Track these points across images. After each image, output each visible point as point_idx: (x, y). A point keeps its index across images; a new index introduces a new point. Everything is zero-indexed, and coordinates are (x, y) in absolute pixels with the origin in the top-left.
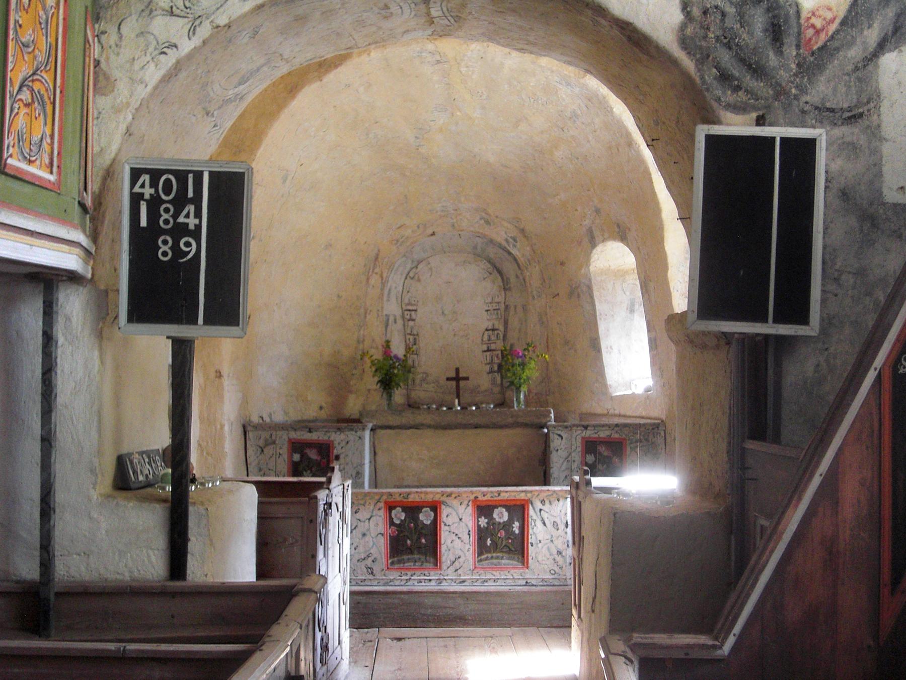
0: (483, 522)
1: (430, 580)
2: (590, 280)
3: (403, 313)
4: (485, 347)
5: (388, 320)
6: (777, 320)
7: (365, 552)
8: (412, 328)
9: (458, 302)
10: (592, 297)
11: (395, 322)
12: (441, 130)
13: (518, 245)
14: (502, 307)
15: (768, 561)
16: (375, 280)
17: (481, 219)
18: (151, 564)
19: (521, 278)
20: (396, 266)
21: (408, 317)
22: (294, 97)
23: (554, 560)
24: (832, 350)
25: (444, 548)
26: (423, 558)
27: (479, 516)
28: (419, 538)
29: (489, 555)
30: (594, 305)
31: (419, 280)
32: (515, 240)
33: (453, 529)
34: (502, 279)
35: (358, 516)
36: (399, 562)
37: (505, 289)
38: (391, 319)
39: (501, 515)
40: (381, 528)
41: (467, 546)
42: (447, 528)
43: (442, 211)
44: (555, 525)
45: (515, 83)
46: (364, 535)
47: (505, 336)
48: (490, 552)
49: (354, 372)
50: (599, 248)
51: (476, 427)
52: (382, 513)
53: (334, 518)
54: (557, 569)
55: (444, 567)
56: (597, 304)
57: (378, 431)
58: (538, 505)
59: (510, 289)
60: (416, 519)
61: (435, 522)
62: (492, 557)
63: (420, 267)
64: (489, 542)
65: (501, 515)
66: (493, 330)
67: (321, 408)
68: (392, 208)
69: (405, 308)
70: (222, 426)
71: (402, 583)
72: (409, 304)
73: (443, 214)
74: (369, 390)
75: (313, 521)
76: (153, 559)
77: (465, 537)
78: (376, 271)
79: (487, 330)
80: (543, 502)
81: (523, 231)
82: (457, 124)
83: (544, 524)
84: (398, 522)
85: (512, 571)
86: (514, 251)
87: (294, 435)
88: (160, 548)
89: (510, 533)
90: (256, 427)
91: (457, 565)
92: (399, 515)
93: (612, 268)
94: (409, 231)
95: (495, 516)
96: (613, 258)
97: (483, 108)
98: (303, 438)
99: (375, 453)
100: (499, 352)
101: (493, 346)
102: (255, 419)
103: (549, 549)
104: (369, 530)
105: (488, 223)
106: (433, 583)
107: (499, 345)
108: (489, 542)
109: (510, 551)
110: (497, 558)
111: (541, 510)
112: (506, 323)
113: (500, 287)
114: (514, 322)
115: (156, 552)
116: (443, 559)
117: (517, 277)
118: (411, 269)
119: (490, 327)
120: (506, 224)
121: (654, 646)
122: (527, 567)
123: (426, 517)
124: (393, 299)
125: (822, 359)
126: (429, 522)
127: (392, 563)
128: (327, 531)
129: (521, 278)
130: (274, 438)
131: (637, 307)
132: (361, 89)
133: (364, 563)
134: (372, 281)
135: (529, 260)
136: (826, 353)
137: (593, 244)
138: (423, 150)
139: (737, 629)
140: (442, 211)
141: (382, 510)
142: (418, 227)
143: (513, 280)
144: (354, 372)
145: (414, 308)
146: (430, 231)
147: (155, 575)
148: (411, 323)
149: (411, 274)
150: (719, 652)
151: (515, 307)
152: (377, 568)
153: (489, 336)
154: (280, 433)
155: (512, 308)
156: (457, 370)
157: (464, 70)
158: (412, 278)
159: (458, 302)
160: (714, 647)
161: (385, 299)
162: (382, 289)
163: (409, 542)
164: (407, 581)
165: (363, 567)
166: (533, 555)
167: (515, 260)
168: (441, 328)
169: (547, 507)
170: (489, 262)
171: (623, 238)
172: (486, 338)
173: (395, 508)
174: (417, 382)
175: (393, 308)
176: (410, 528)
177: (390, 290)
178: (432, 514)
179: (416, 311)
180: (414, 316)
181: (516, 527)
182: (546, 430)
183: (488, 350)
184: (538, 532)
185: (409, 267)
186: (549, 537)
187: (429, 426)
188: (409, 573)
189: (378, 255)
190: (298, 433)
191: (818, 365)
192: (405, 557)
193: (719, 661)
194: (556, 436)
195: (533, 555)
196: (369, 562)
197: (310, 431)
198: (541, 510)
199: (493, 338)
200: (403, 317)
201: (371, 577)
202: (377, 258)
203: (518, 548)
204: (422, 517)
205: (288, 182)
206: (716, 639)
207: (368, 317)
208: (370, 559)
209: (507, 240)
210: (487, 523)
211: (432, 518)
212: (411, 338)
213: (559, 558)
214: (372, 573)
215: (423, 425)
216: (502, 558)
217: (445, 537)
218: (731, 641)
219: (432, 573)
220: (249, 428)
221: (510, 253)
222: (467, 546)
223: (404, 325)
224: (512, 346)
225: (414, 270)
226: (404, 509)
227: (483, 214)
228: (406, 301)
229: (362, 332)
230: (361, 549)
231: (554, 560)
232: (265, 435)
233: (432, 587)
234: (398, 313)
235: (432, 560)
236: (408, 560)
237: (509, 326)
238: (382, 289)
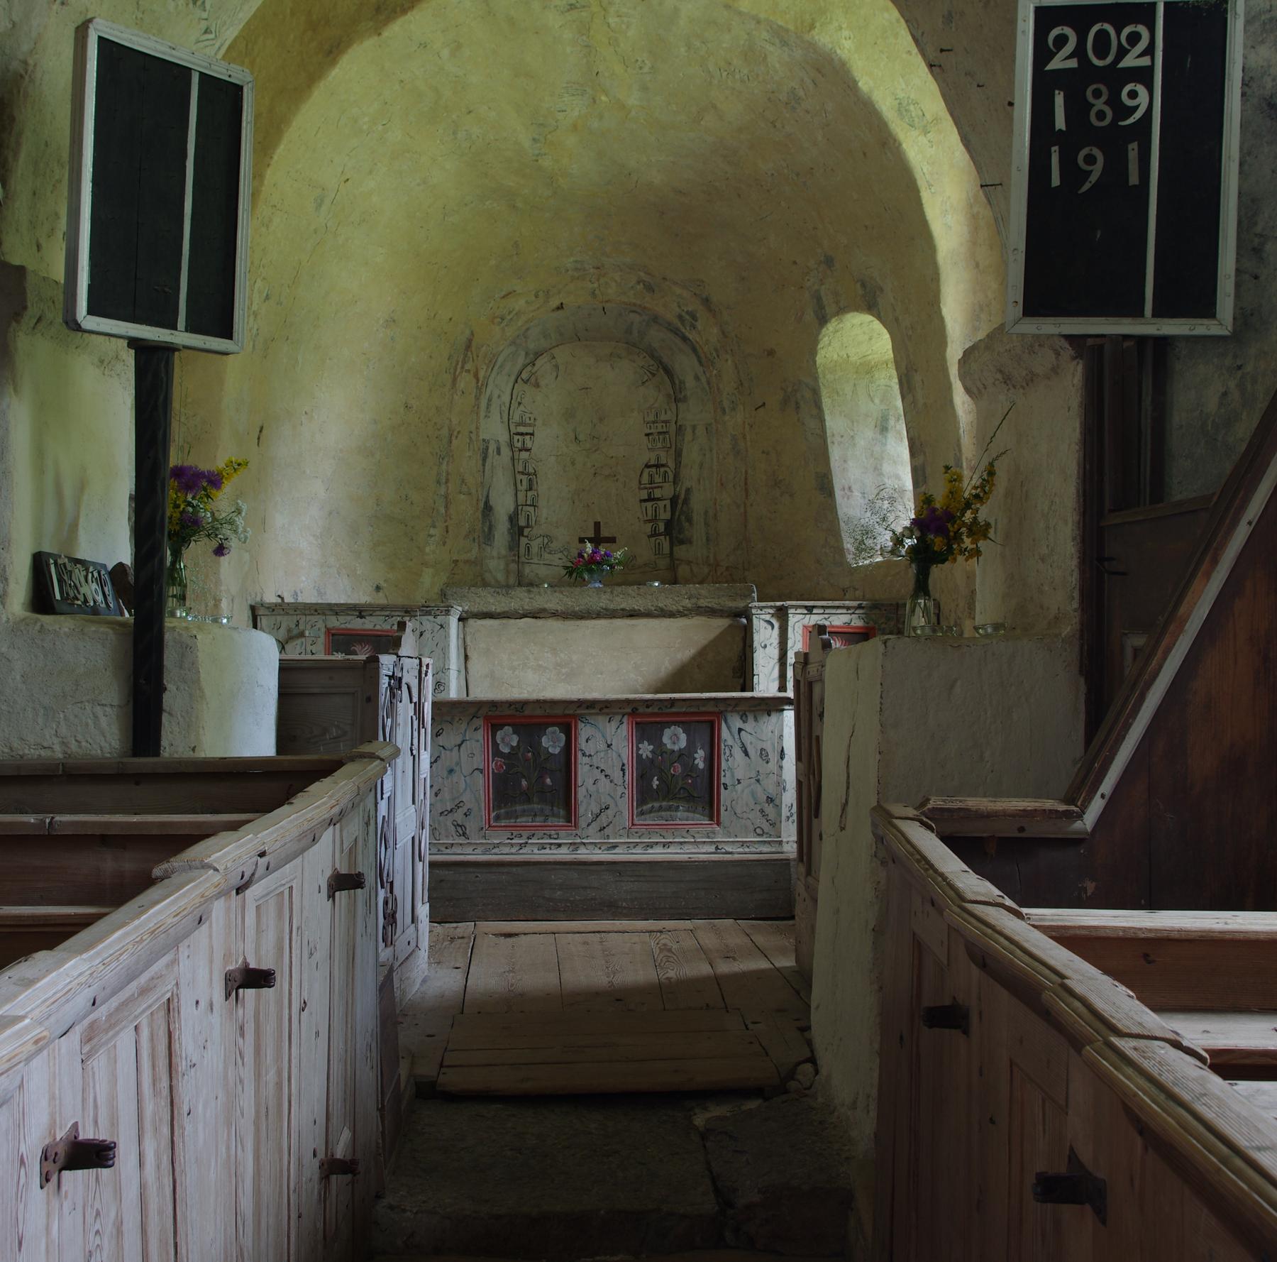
0: (646, 749)
1: (559, 845)
2: (816, 379)
3: (511, 439)
4: (644, 495)
5: (487, 448)
6: (1156, 314)
7: (453, 799)
8: (526, 462)
9: (601, 420)
10: (818, 405)
11: (499, 453)
12: (575, 127)
13: (699, 325)
14: (673, 428)
15: (1160, 667)
16: (465, 381)
17: (638, 283)
18: (99, 733)
19: (703, 380)
20: (501, 359)
21: (520, 445)
22: (333, 63)
23: (762, 811)
24: (1249, 368)
25: (581, 793)
26: (547, 808)
27: (640, 741)
28: (541, 777)
29: (656, 805)
30: (822, 421)
31: (537, 385)
32: (694, 318)
33: (595, 761)
34: (673, 383)
35: (441, 740)
36: (508, 816)
37: (676, 400)
38: (492, 447)
39: (675, 739)
40: (479, 761)
41: (620, 790)
42: (586, 760)
43: (576, 269)
44: (763, 753)
45: (698, 44)
46: (451, 771)
47: (676, 476)
48: (656, 800)
49: (432, 531)
50: (831, 326)
51: (633, 614)
52: (480, 735)
53: (405, 710)
54: (766, 826)
55: (583, 823)
56: (827, 417)
57: (471, 622)
58: (736, 722)
59: (685, 400)
60: (535, 747)
61: (568, 749)
62: (660, 809)
63: (539, 363)
64: (655, 783)
65: (675, 739)
66: (657, 466)
67: (378, 588)
68: (493, 262)
69: (513, 430)
70: (217, 602)
71: (513, 850)
72: (518, 425)
73: (576, 274)
74: (456, 562)
75: (372, 699)
76: (103, 721)
77: (617, 775)
78: (467, 367)
79: (647, 466)
80: (744, 718)
81: (706, 301)
82: (601, 117)
83: (746, 753)
84: (506, 750)
85: (693, 830)
86: (691, 335)
87: (335, 622)
88: (116, 702)
89: (690, 769)
90: (272, 609)
91: (603, 819)
92: (509, 739)
93: (853, 359)
94: (522, 302)
95: (666, 740)
96: (859, 342)
97: (644, 88)
98: (349, 626)
99: (466, 657)
100: (668, 503)
101: (657, 493)
102: (271, 598)
103: (753, 794)
104: (458, 764)
105: (650, 288)
106: (564, 850)
107: (667, 491)
108: (655, 783)
109: (690, 798)
110: (669, 809)
111: (740, 730)
112: (678, 454)
113: (669, 396)
114: (692, 453)
115: (108, 709)
116: (581, 810)
117: (697, 378)
118: (526, 366)
119: (652, 462)
120: (678, 291)
121: (967, 814)
122: (718, 824)
123: (552, 742)
124: (495, 410)
125: (1232, 384)
126: (557, 751)
127: (498, 818)
128: (395, 725)
129: (703, 380)
130: (301, 627)
131: (892, 422)
132: (445, 53)
133: (450, 817)
134: (461, 385)
135: (716, 350)
136: (1240, 373)
137: (823, 320)
138: (546, 163)
139: (1107, 786)
140: (576, 269)
141: (481, 732)
142: (536, 296)
143: (690, 383)
144: (432, 531)
145: (529, 430)
146: (556, 303)
147: (107, 749)
148: (524, 455)
149: (524, 376)
150: (1078, 825)
151: (694, 428)
152: (471, 826)
153: (651, 476)
154: (314, 618)
155: (689, 430)
156: (597, 525)
157: (612, 20)
158: (526, 382)
159: (601, 420)
160: (1067, 814)
161: (482, 414)
162: (477, 398)
163: (524, 783)
164: (521, 846)
165: (449, 824)
166: (728, 803)
167: (694, 350)
168: (573, 463)
169: (749, 726)
170: (652, 357)
171: (870, 306)
172: (645, 479)
173: (501, 726)
174: (535, 550)
175: (494, 429)
176: (527, 760)
177: (490, 400)
178: (563, 736)
179: (532, 434)
180: (529, 444)
181: (700, 758)
182: (744, 621)
183: (650, 499)
184: (734, 765)
185: (521, 360)
186: (753, 774)
187: (555, 615)
188: (525, 834)
189: (470, 341)
190: (342, 619)
191: (1225, 394)
192: (519, 808)
193: (1075, 842)
194: (763, 624)
195: (728, 803)
196: (459, 816)
197: (361, 617)
198: (740, 730)
199: (658, 479)
200: (511, 445)
201: (462, 840)
202: (468, 346)
203: (703, 793)
204: (545, 742)
205: (324, 208)
206: (1070, 800)
207: (454, 441)
208: (461, 811)
209: (680, 317)
210: (652, 752)
211: (562, 744)
212: (525, 478)
213: (769, 809)
214: (464, 834)
215: (544, 610)
216: (677, 809)
217: (584, 773)
218: (1096, 807)
219: (562, 833)
220: (261, 612)
221: (685, 339)
222: (620, 790)
223: (513, 459)
224: (688, 491)
225: (529, 368)
226: (517, 729)
227: (642, 274)
228: (516, 418)
229: (444, 467)
230: (446, 795)
231: (762, 811)
232: (287, 622)
233: (563, 854)
234: (503, 437)
235: (562, 812)
236: (524, 813)
237: (684, 460)
238: (477, 398)
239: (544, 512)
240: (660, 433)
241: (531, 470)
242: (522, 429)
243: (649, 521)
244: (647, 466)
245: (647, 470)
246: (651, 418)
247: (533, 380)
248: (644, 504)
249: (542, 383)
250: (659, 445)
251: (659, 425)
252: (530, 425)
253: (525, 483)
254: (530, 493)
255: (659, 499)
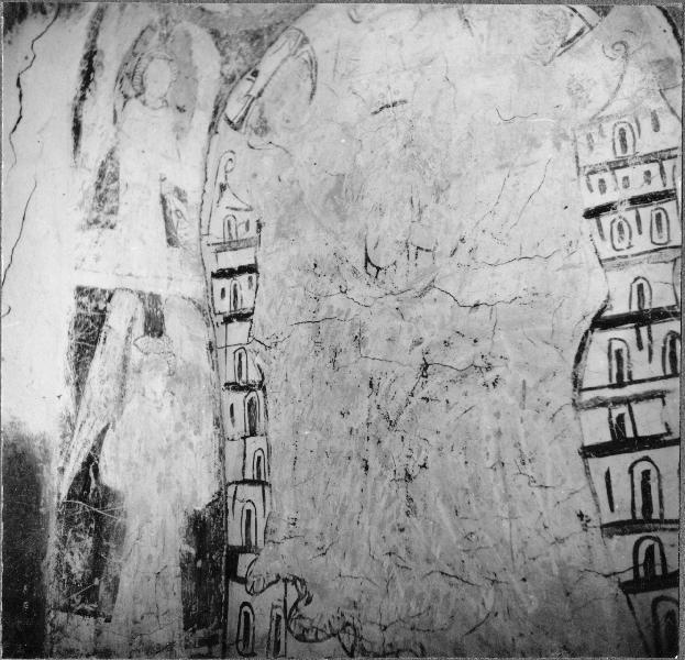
4: (597, 428)
9: (439, 191)
21: (224, 306)
31: (263, 128)
63: (267, 66)
79: (601, 322)
119: (620, 307)
148: (238, 331)
149: (234, 110)
158: (235, 127)
168: (358, 340)
172: (597, 368)
179: (251, 269)
180: (246, 303)
212: (238, 399)
225: (244, 86)
228: (217, 233)
239: (285, 503)
240: (638, 201)
241: (254, 377)
242: (231, 260)
243: (619, 528)
244: (601, 322)
245: (601, 338)
246: (605, 154)
247: (253, 118)
248: (599, 465)
249: (275, 118)
250: (642, 243)
251: (635, 173)
252: (247, 244)
253: (240, 412)
254: (254, 444)
255: (655, 442)
